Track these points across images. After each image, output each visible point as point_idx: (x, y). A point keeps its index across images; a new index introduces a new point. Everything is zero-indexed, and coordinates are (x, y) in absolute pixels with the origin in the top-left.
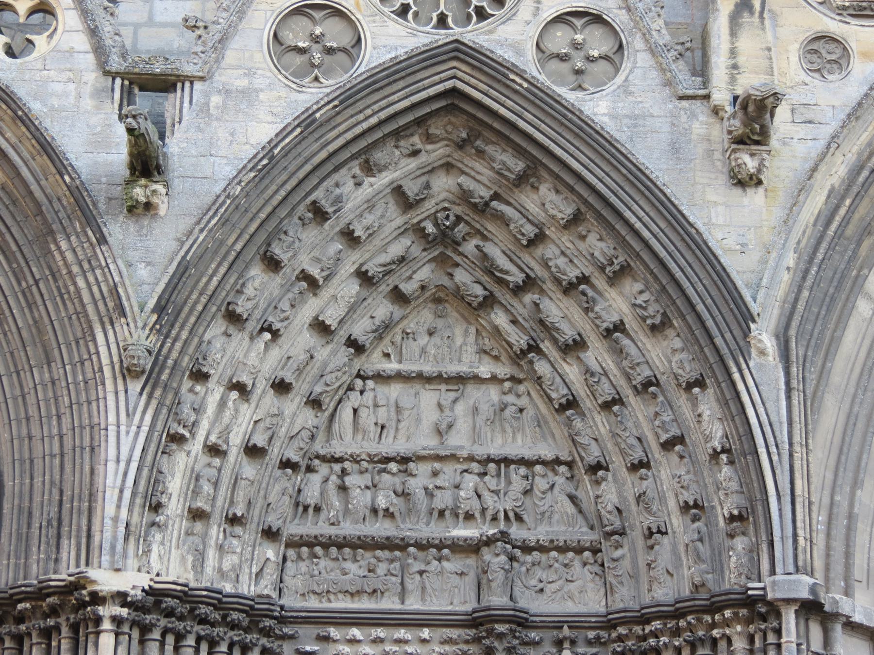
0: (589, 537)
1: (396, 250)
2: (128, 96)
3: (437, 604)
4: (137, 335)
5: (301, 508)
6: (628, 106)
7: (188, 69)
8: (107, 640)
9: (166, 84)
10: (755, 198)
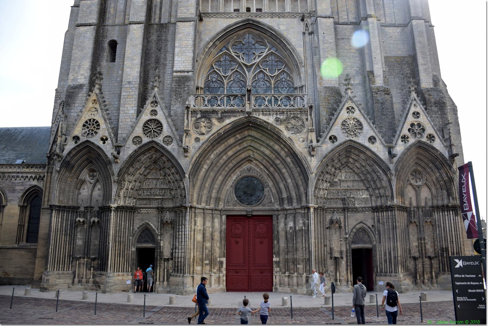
0: (171, 197)
1: (149, 164)
2: (116, 148)
3: (154, 206)
4: (116, 178)
5: (139, 195)
6: (172, 148)
7: (123, 145)
8: (113, 212)
9: (121, 146)
10: (187, 158)
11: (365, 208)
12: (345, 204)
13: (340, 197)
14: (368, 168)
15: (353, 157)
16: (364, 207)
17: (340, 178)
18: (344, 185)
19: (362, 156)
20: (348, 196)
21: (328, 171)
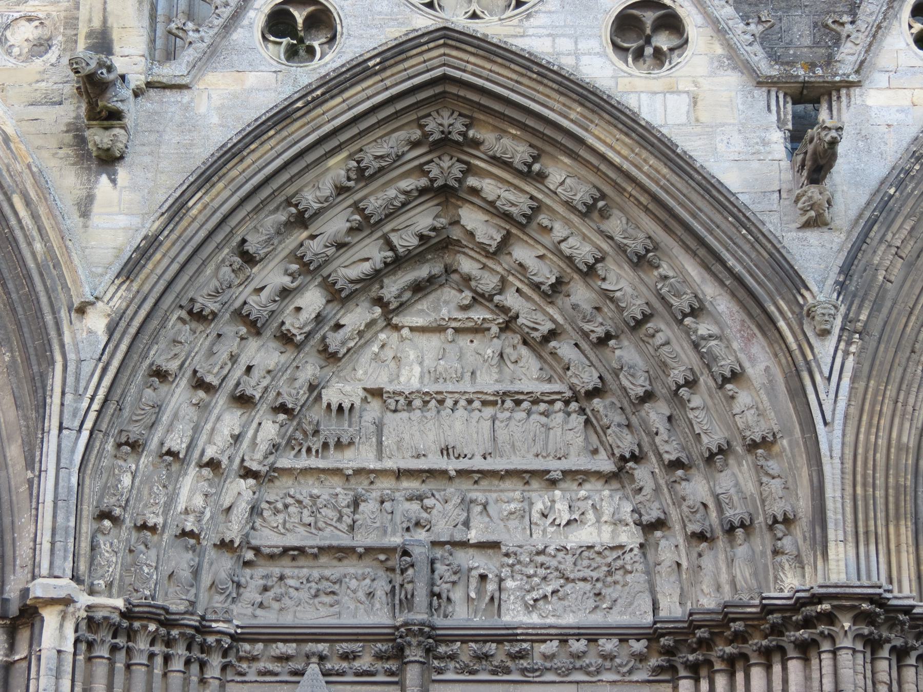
11: (592, 636)
12: (408, 602)
13: (362, 540)
14: (620, 279)
15: (489, 188)
16: (579, 633)
17: (381, 380)
18: (416, 439)
19: (559, 173)
20: (443, 530)
21: (257, 305)
